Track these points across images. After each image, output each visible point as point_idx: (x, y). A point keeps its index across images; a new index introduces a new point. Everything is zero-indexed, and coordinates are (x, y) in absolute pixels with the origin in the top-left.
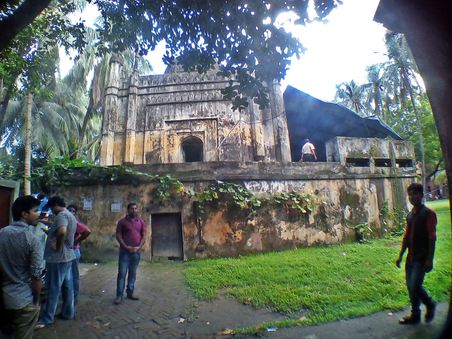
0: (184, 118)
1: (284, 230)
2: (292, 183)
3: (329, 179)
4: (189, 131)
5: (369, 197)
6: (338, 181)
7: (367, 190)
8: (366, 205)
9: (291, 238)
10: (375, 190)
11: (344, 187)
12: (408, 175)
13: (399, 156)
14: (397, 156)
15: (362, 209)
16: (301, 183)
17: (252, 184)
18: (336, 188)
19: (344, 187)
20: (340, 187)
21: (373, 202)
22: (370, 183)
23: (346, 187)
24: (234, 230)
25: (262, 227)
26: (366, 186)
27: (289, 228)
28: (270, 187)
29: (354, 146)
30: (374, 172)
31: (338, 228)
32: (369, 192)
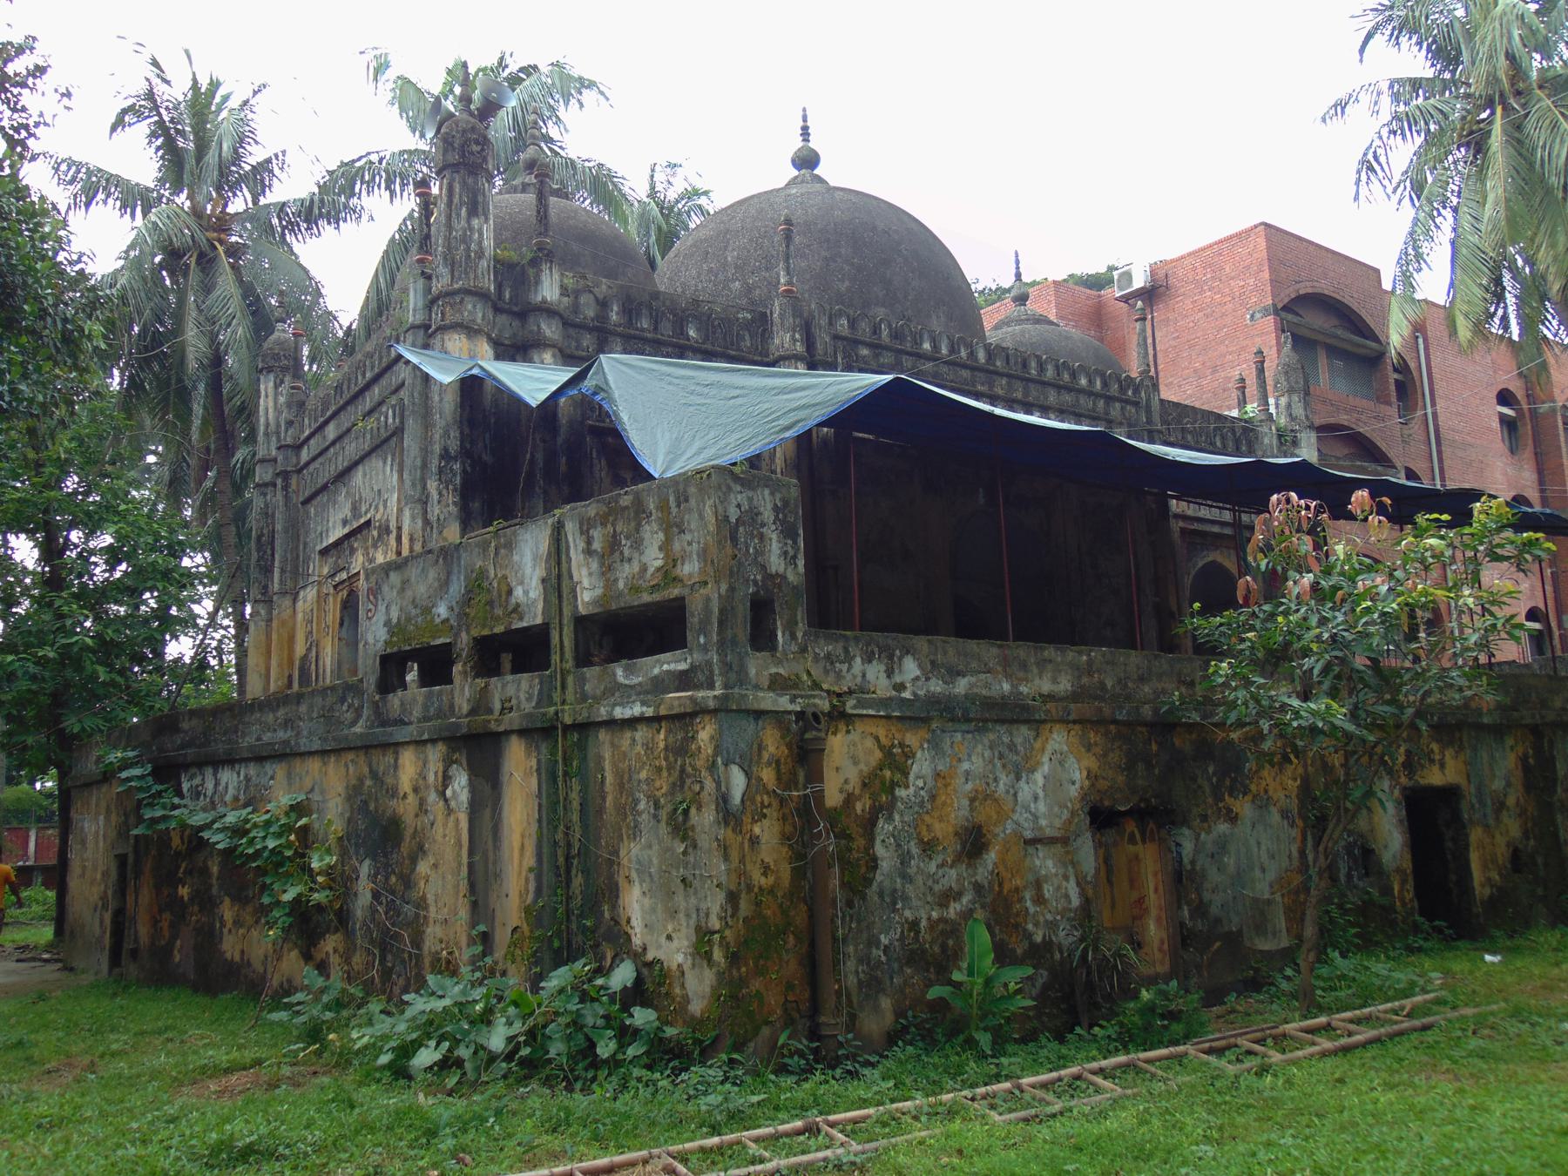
0: (337, 533)
1: (229, 925)
2: (252, 769)
3: (323, 753)
4: (344, 575)
5: (439, 830)
6: (351, 756)
7: (432, 797)
8: (423, 867)
9: (237, 958)
10: (464, 796)
11: (361, 780)
12: (637, 710)
13: (599, 592)
14: (588, 592)
15: (408, 882)
16: (269, 768)
17: (191, 778)
18: (340, 788)
19: (361, 780)
20: (354, 782)
21: (449, 854)
22: (448, 762)
23: (368, 782)
24: (161, 911)
25: (196, 908)
26: (431, 778)
27: (238, 923)
28: (217, 784)
29: (409, 593)
30: (465, 708)
31: (335, 951)
32: (441, 803)
